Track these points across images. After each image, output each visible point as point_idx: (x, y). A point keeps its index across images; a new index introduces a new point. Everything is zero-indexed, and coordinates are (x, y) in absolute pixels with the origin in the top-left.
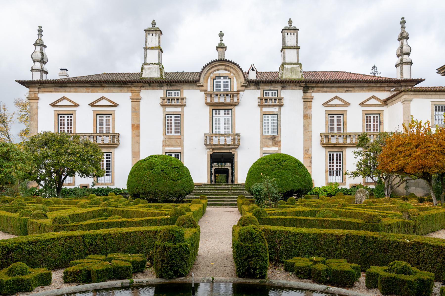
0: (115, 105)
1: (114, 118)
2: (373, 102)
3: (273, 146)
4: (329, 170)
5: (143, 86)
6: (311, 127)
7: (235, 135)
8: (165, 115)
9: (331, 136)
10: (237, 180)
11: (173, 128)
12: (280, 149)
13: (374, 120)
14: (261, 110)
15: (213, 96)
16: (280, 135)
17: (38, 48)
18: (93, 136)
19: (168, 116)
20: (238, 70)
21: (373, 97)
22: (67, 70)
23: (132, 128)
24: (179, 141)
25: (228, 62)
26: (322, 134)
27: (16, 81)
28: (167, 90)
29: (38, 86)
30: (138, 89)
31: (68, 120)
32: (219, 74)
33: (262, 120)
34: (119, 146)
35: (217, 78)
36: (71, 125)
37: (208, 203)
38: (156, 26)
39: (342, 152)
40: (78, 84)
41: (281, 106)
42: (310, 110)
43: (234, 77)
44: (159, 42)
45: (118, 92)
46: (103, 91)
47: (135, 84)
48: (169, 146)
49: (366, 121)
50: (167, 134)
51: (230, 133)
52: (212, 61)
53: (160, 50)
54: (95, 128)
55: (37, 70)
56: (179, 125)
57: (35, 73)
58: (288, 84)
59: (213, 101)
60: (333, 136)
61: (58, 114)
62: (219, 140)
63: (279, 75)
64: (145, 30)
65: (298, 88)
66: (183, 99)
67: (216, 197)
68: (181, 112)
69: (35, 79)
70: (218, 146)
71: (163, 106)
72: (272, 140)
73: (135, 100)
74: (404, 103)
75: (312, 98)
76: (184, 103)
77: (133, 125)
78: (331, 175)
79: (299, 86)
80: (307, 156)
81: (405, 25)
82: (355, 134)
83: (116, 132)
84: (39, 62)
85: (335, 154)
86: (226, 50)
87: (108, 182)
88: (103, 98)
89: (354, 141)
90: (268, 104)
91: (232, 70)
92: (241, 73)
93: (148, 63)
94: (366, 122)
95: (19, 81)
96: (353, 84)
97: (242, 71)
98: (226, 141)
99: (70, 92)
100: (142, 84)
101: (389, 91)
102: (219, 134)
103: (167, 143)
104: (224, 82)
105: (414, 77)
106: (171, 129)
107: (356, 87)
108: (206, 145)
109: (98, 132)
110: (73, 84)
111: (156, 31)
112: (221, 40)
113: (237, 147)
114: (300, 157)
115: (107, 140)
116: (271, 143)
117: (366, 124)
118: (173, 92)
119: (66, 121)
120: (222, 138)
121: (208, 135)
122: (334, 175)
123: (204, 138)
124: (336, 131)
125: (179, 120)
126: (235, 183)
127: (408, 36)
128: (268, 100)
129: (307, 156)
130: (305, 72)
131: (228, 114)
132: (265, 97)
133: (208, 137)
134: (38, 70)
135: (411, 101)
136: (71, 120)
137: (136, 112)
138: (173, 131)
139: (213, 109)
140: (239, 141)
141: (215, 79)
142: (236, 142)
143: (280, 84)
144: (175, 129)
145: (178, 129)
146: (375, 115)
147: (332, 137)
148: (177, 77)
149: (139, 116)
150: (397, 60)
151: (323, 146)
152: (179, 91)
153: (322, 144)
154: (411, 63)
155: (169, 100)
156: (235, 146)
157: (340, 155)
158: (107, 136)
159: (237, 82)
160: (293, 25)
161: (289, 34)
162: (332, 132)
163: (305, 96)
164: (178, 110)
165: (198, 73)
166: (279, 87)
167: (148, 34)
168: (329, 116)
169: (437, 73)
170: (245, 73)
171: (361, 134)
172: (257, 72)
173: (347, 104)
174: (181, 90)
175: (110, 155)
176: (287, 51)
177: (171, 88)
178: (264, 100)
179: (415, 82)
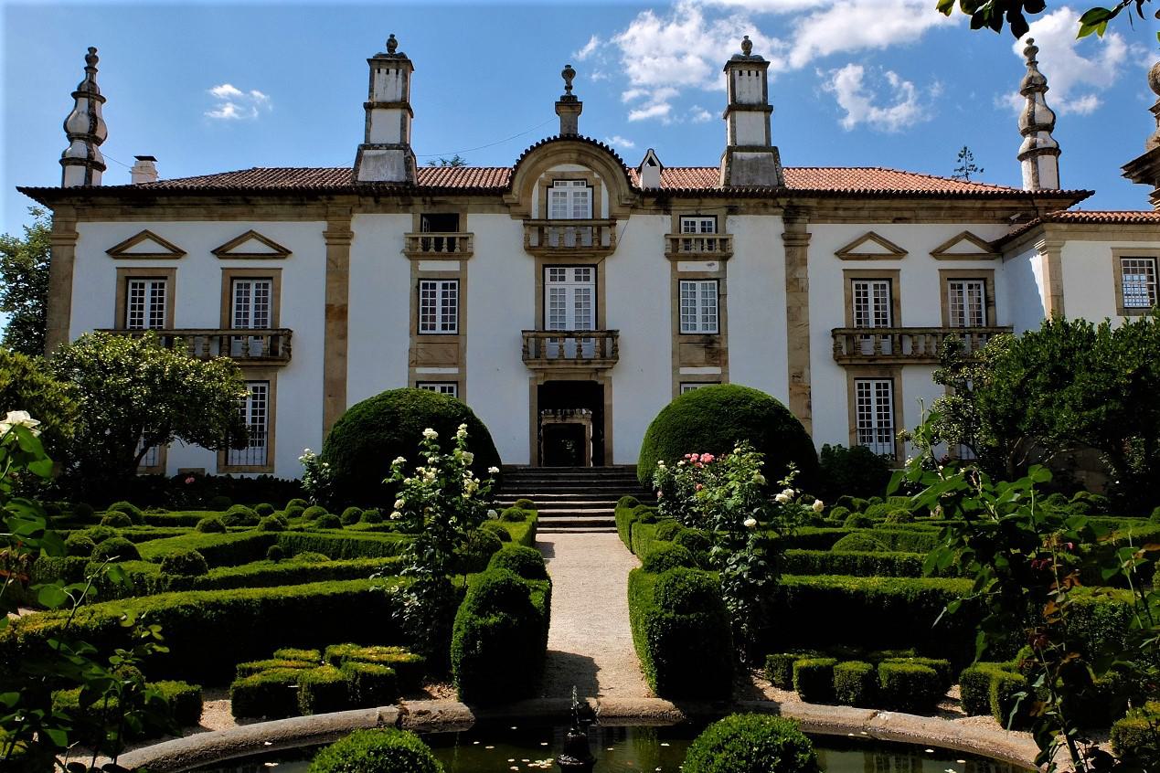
0: (283, 253)
2: (966, 247)
3: (709, 363)
5: (360, 205)
9: (861, 337)
11: (439, 314)
12: (725, 373)
14: (674, 268)
15: (546, 231)
17: (84, 102)
19: (423, 286)
21: (968, 236)
22: (155, 160)
23: (326, 315)
24: (453, 352)
26: (837, 332)
27: (20, 189)
31: (154, 293)
32: (563, 173)
33: (677, 295)
35: (557, 184)
36: (161, 307)
38: (397, 51)
41: (725, 259)
42: (804, 267)
43: (602, 182)
44: (405, 91)
45: (290, 217)
46: (251, 216)
47: (339, 199)
48: (426, 365)
50: (421, 331)
52: (543, 141)
54: (228, 313)
57: (71, 168)
58: (748, 200)
60: (867, 336)
61: (128, 278)
62: (561, 347)
63: (719, 177)
64: (369, 60)
65: (772, 210)
66: (467, 238)
68: (460, 272)
69: (69, 184)
70: (559, 363)
71: (412, 256)
72: (705, 347)
73: (338, 241)
77: (329, 308)
79: (774, 207)
80: (800, 390)
81: (1038, 57)
82: (924, 331)
83: (281, 327)
84: (83, 139)
85: (873, 385)
88: (251, 234)
89: (921, 350)
90: (693, 251)
91: (595, 163)
93: (373, 145)
95: (27, 188)
96: (914, 201)
98: (579, 350)
99: (162, 218)
100: (356, 198)
102: (561, 331)
104: (576, 194)
105: (1067, 187)
106: (433, 319)
107: (922, 208)
109: (233, 326)
110: (172, 198)
112: (569, 87)
114: (782, 396)
116: (701, 354)
119: (147, 297)
120: (571, 341)
124: (872, 325)
125: (453, 294)
127: (1045, 83)
128: (693, 241)
129: (800, 390)
134: (81, 159)
136: (161, 293)
137: (337, 272)
138: (439, 323)
139: (545, 266)
141: (552, 187)
142: (608, 354)
143: (722, 202)
144: (444, 319)
145: (452, 319)
149: (347, 281)
151: (840, 362)
157: (886, 386)
158: (257, 337)
160: (754, 52)
161: (745, 72)
162: (863, 325)
163: (787, 232)
164: (453, 266)
167: (376, 71)
168: (854, 283)
169: (1124, 175)
171: (937, 331)
172: (662, 168)
175: (263, 389)
176: (739, 115)
179: (1071, 198)
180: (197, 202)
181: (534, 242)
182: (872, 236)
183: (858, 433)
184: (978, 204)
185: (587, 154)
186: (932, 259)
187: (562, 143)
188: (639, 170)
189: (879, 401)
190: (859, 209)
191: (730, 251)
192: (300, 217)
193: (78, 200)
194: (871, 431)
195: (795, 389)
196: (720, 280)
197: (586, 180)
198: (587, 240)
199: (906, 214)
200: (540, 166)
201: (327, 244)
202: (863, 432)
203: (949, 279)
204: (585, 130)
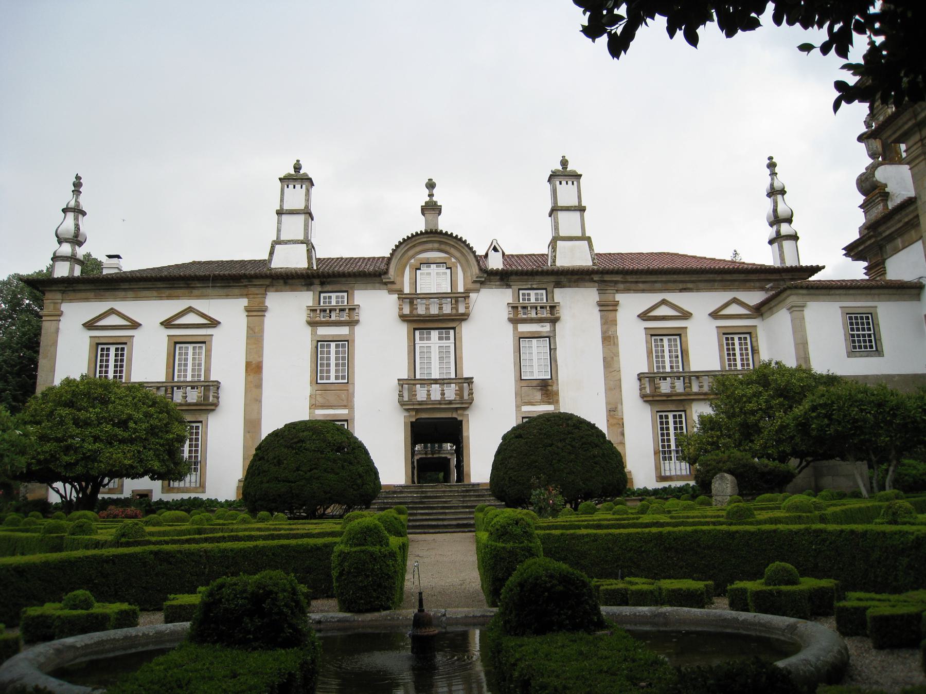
0: (214, 323)
1: (210, 350)
2: (734, 309)
3: (543, 402)
4: (661, 449)
7: (463, 381)
8: (315, 343)
10: (469, 476)
11: (333, 368)
13: (740, 344)
14: (515, 329)
16: (557, 380)
18: (166, 387)
19: (320, 344)
20: (466, 250)
21: (735, 301)
22: (121, 258)
23: (246, 370)
25: (446, 237)
26: (642, 376)
28: (320, 292)
29: (64, 289)
30: (262, 290)
31: (116, 355)
32: (428, 258)
33: (518, 350)
34: (218, 408)
36: (122, 366)
37: (410, 524)
38: (302, 172)
39: (685, 411)
40: (141, 283)
45: (220, 297)
46: (190, 297)
48: (323, 407)
49: (725, 347)
50: (319, 381)
51: (453, 376)
53: (308, 215)
54: (171, 370)
55: (64, 258)
56: (347, 363)
59: (415, 312)
61: (98, 344)
62: (428, 391)
64: (280, 179)
66: (354, 309)
67: (427, 511)
70: (427, 404)
71: (313, 324)
72: (541, 390)
74: (791, 311)
75: (616, 304)
76: (356, 318)
77: (248, 364)
78: (666, 460)
81: (777, 170)
82: (708, 373)
83: (212, 379)
85: (671, 415)
86: (440, 214)
87: (193, 485)
88: (190, 310)
89: (706, 389)
91: (452, 251)
92: (471, 258)
94: (725, 350)
97: (474, 253)
98: (443, 394)
99: (124, 299)
101: (762, 289)
102: (428, 380)
103: (319, 399)
105: (804, 263)
106: (328, 371)
107: (700, 281)
108: (402, 403)
109: (176, 379)
110: (132, 283)
111: (302, 179)
112: (431, 195)
113: (467, 406)
115: (193, 396)
116: (538, 395)
117: (726, 352)
118: (334, 295)
120: (436, 388)
121: (405, 382)
122: (670, 459)
123: (397, 388)
126: (466, 482)
128: (529, 308)
130: (601, 254)
131: (448, 338)
133: (406, 386)
134: (66, 257)
135: (803, 307)
136: (122, 355)
137: (255, 337)
138: (333, 374)
140: (471, 394)
141: (420, 269)
142: (466, 396)
143: (552, 278)
144: (337, 371)
146: (742, 336)
147: (662, 381)
148: (340, 267)
150: (771, 232)
151: (645, 399)
152: (345, 294)
153: (643, 396)
154: (795, 237)
155: (325, 311)
156: (462, 403)
157: (680, 416)
158: (193, 388)
159: (464, 274)
161: (564, 183)
164: (344, 331)
165: (383, 258)
166: (548, 282)
167: (286, 186)
168: (653, 338)
169: (845, 255)
170: (481, 256)
171: (717, 373)
172: (503, 254)
173: (686, 315)
174: (350, 291)
176: (561, 215)
177: (328, 288)
178: (519, 308)
180: (149, 286)
181: (407, 310)
183: (661, 454)
185: (446, 243)
186: (710, 319)
187: (427, 236)
190: (655, 282)
191: (557, 315)
192: (227, 296)
193: (63, 287)
194: (670, 452)
195: (611, 421)
196: (551, 337)
197: (445, 263)
198: (447, 309)
200: (411, 253)
201: (247, 316)
202: (664, 452)
203: (724, 334)
204: (445, 224)
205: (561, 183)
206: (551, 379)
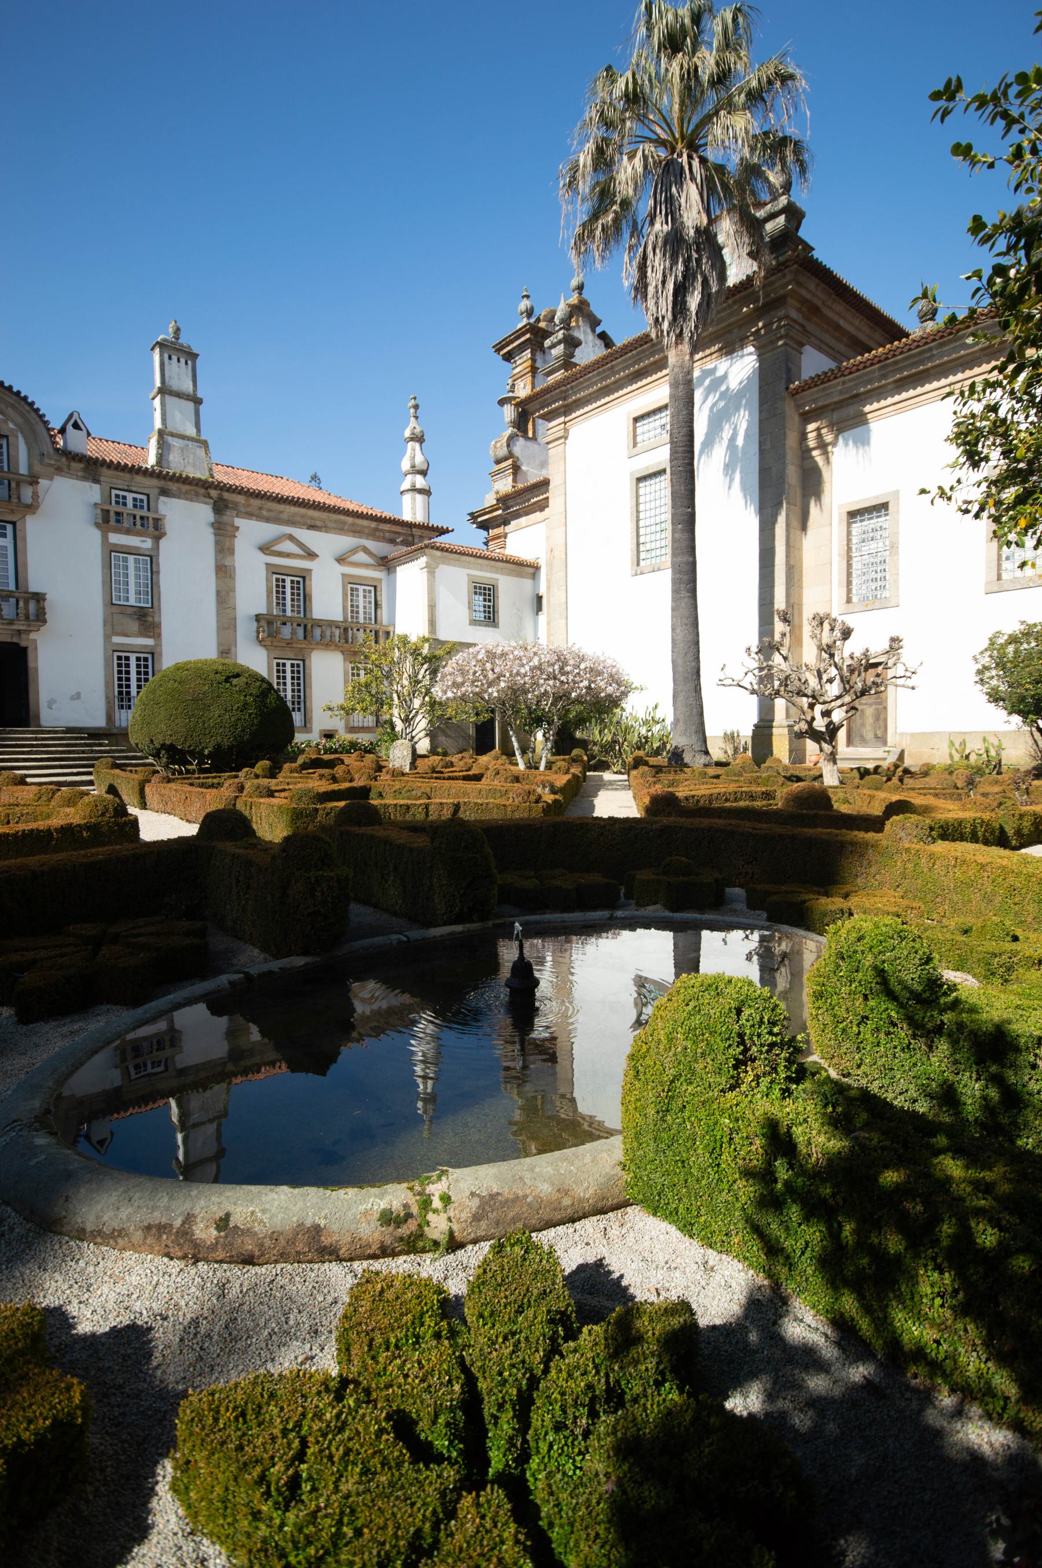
2: (361, 557)
6: (235, 598)
14: (105, 538)
16: (160, 610)
33: (108, 565)
72: (139, 619)
82: (331, 624)
91: (10, 411)
105: (435, 522)
116: (134, 626)
132: (114, 508)
143: (154, 482)
159: (29, 449)
161: (175, 358)
168: (275, 576)
182: (291, 538)
184: (373, 525)
188: (62, 431)
189: (293, 678)
196: (153, 558)
199: (318, 523)
205: (170, 358)
206: (152, 607)
